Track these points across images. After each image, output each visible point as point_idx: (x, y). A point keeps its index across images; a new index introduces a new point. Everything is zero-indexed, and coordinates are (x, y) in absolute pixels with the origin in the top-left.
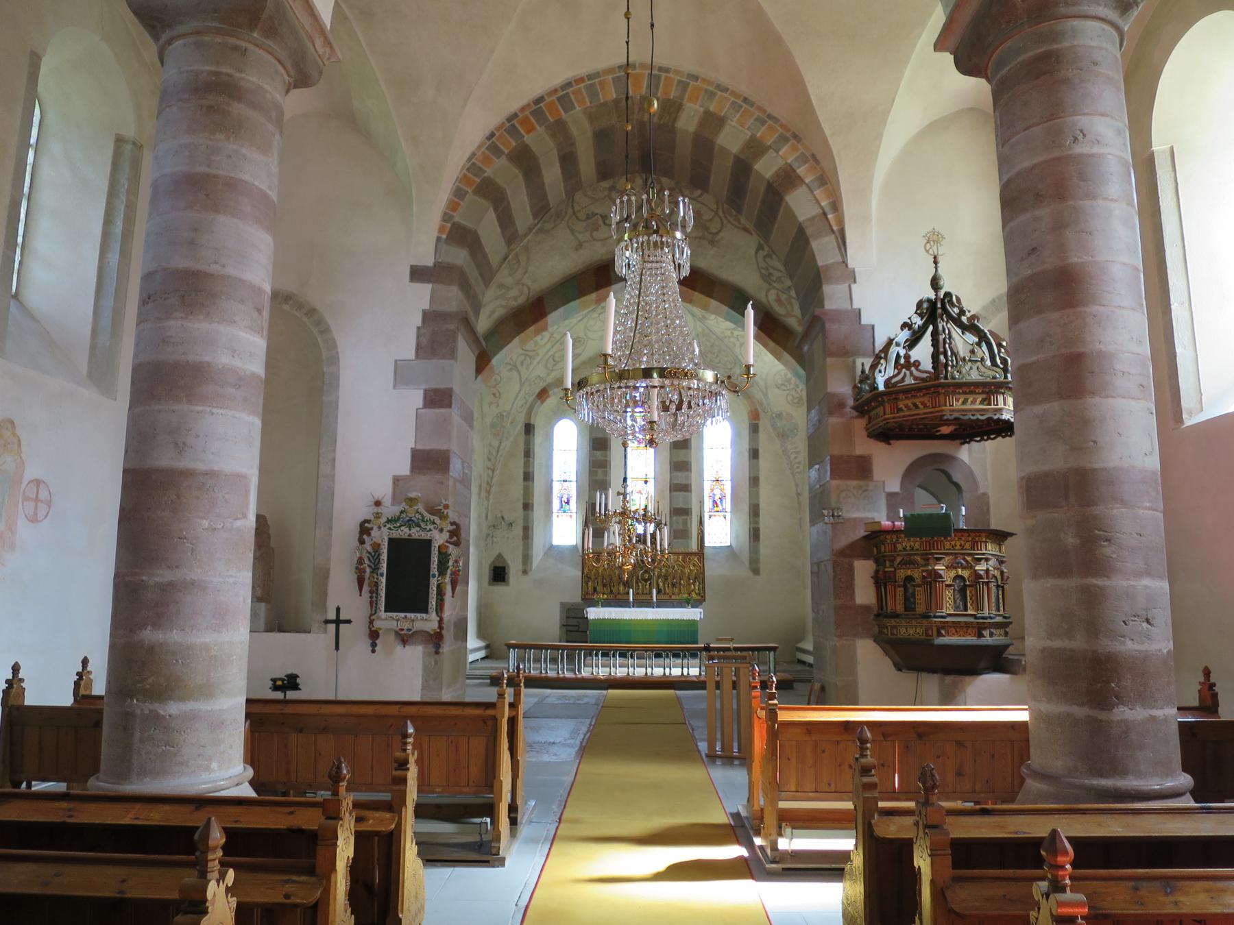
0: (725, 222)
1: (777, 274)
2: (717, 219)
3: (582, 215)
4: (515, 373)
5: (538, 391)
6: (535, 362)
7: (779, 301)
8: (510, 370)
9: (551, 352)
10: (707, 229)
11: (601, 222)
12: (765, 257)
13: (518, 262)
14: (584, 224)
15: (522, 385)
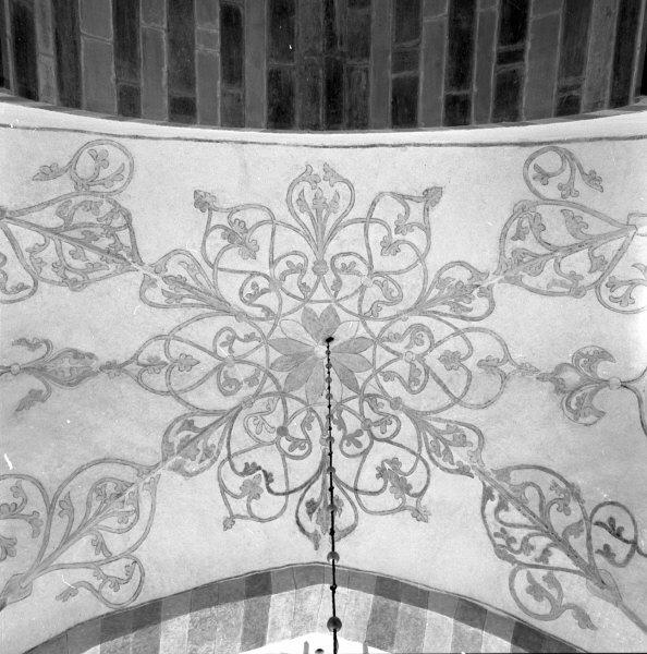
1: (519, 534)
3: (241, 468)
7: (534, 589)
10: (407, 488)
11: (263, 484)
12: (497, 510)
13: (137, 511)
14: (240, 480)
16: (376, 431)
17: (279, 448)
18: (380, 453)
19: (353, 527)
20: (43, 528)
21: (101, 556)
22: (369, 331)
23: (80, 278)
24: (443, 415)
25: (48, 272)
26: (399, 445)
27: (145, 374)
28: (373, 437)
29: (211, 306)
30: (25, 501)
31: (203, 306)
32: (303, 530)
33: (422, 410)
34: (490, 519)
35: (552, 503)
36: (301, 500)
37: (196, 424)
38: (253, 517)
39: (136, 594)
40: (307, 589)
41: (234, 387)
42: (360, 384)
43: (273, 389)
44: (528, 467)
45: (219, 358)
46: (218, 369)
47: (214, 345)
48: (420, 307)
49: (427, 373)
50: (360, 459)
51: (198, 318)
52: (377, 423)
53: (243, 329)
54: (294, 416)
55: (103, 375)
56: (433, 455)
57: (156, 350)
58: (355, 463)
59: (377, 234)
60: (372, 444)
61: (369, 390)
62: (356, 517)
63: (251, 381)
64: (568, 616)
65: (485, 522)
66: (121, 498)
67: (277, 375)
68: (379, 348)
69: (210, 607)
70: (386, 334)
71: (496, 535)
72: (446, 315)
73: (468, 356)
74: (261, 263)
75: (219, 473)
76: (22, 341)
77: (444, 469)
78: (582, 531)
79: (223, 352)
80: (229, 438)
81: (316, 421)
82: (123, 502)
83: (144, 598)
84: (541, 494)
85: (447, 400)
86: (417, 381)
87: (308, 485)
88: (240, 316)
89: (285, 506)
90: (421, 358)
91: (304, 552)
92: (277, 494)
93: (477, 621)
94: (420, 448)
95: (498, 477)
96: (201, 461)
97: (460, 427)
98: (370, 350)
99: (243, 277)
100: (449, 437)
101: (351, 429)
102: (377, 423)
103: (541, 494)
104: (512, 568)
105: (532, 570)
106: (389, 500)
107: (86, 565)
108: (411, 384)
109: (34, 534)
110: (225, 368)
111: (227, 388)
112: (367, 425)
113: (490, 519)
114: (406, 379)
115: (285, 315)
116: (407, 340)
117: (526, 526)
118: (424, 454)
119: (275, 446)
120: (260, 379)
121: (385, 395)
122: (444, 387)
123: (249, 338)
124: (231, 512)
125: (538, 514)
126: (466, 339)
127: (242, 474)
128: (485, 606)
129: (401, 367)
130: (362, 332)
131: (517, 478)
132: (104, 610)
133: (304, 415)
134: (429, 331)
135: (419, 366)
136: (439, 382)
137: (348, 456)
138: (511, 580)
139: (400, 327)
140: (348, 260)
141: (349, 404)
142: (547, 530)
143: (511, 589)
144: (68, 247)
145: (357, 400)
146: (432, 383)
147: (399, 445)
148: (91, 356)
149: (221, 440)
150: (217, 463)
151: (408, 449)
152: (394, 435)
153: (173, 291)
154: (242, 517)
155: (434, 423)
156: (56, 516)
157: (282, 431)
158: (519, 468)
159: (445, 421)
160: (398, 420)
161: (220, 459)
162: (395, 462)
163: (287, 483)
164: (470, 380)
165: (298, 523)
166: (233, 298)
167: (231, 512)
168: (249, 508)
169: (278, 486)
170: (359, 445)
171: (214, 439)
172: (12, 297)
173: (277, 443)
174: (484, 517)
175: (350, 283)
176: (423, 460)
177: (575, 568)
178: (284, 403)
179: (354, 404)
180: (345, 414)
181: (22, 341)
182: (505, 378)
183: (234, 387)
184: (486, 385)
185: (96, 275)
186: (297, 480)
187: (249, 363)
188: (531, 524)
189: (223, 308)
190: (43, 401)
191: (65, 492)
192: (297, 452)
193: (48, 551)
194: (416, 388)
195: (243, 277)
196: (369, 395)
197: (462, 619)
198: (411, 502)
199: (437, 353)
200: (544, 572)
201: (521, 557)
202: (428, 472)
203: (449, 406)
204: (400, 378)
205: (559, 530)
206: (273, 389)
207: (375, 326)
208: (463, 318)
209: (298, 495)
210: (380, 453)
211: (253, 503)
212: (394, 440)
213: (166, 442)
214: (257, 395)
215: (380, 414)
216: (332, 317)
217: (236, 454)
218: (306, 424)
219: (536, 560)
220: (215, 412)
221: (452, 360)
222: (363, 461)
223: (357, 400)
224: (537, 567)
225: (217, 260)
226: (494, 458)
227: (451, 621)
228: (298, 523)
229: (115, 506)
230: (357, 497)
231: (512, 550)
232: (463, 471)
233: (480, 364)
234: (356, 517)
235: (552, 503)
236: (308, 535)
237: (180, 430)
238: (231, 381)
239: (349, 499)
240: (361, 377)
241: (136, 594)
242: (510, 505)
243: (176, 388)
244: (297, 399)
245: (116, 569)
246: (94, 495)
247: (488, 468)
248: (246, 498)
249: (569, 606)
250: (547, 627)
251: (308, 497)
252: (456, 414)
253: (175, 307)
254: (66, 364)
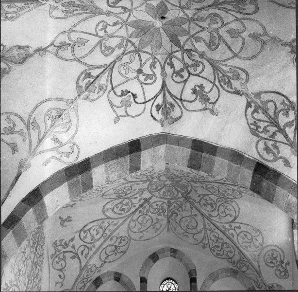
0: (221, 89)
1: (262, 125)
2: (215, 88)
3: (119, 93)
4: (76, 260)
5: (94, 278)
6: (91, 253)
7: (267, 149)
8: (73, 258)
9: (104, 246)
11: (132, 99)
13: (70, 122)
14: (120, 99)
15: (81, 270)
16: (191, 70)
17: (139, 80)
18: (194, 82)
19: (180, 117)
20: (27, 137)
21: (58, 145)
22: (186, 15)
23: (14, 15)
24: (227, 63)
26: (203, 78)
27: (60, 51)
28: (189, 73)
29: (92, 12)
30: (14, 125)
31: (86, 13)
32: (155, 119)
33: (217, 59)
34: (249, 116)
35: (281, 111)
36: (153, 105)
37: (92, 74)
38: (128, 115)
39: (77, 157)
40: (159, 147)
41: (110, 51)
42: (182, 44)
43: (132, 49)
44: (271, 92)
45: (100, 37)
46: (100, 43)
47: (96, 31)
49: (219, 39)
50: (183, 84)
51: (86, 19)
52: (191, 66)
53: (111, 20)
54: (145, 62)
55: (36, 55)
56: (222, 83)
57: (64, 38)
58: (180, 86)
60: (189, 77)
61: (186, 47)
62: (182, 112)
63: (119, 46)
64: (281, 161)
65: (246, 117)
66: (61, 117)
67: (133, 40)
68: (192, 24)
69: (113, 160)
70: (196, 17)
71: (251, 124)
72: (231, 10)
73: (243, 32)
75: (108, 97)
77: (227, 91)
78: (293, 125)
79: (102, 33)
80: (111, 79)
81: (158, 63)
82: (62, 119)
83: (81, 159)
84: (275, 106)
85: (230, 54)
86: (214, 44)
87: (156, 97)
88: (108, 14)
89: (145, 109)
90: (217, 30)
91: (156, 129)
92: (140, 103)
93: (238, 162)
94: (215, 79)
95: (255, 97)
96: (98, 92)
97: (237, 69)
98: (187, 25)
100: (230, 75)
101: (178, 68)
102: (191, 66)
103: (275, 106)
104: (258, 139)
105: (266, 141)
106: (198, 105)
107: (53, 149)
108: (212, 45)
109: (24, 140)
110: (104, 42)
111: (106, 52)
112: (186, 66)
113: (249, 116)
114: (208, 41)
115: (135, 8)
116: (208, 21)
117: (266, 121)
118: (217, 83)
119: (136, 79)
120: (124, 44)
121: (196, 51)
122: (229, 48)
123: (115, 24)
124: (117, 115)
125: (273, 116)
126: (243, 24)
127: (120, 96)
128: (244, 154)
129: (205, 35)
130: (181, 14)
131: (265, 97)
132: (65, 166)
133: (151, 61)
134: (221, 18)
135: (215, 35)
136: (227, 44)
137: (176, 82)
138: (257, 144)
139: (204, 14)
141: (175, 54)
142: (275, 123)
143: (257, 148)
145: (180, 52)
146: (222, 45)
147: (203, 78)
148: (28, 47)
149: (107, 80)
150: (107, 92)
151: (209, 80)
152: (201, 72)
153: (68, 9)
154: (123, 116)
155: (223, 67)
156: (31, 130)
157: (140, 71)
158: (266, 92)
159: (229, 66)
160: (203, 64)
161: (108, 90)
162: (201, 87)
163: (145, 98)
164: (243, 44)
165: (152, 116)
167: (117, 115)
168: (126, 112)
169: (140, 99)
170: (182, 77)
171: (103, 80)
173: (137, 77)
174: (246, 115)
176: (216, 86)
177: (286, 142)
178: (139, 56)
179: (179, 55)
180: (174, 60)
182: (264, 43)
183: (110, 51)
184: (253, 47)
185: (23, 12)
186: (150, 94)
187: (117, 36)
188: (269, 121)
190: (8, 74)
191: (32, 118)
192: (149, 81)
193: (33, 148)
194: (213, 47)
196: (187, 50)
197: (232, 161)
198: (210, 106)
199: (225, 29)
200: (273, 142)
201: (262, 135)
202: (219, 92)
203: (231, 58)
204: (204, 41)
205: (282, 124)
206: (132, 49)
208: (241, 13)
209: (151, 102)
210: (194, 82)
211: (128, 109)
212: (201, 75)
213: (78, 86)
214: (123, 54)
215: (193, 60)
216: (164, 7)
217: (116, 86)
218: (152, 66)
219: (269, 136)
220: (101, 67)
221: (234, 33)
222: (185, 85)
223: (180, 52)
224: (269, 140)
226: (254, 87)
227: (227, 161)
228: (152, 116)
229: (59, 121)
230: (182, 103)
231: (258, 131)
232: (237, 92)
233: (250, 36)
234: (182, 112)
235: (281, 111)
236: (157, 121)
237: (84, 79)
238: (108, 48)
239: (178, 104)
240: (182, 39)
241: (77, 157)
242: (259, 111)
243: (78, 57)
244: (147, 53)
245: (66, 148)
246: (47, 118)
247: (250, 92)
248: (124, 107)
249: (281, 157)
250: (271, 165)
251: (156, 103)
252: (236, 62)
253: (70, 16)
254: (15, 52)
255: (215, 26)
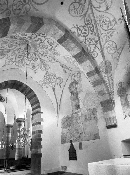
22: (20, 46)
25: (56, 79)
48: (9, 50)
51: (44, 61)
53: (40, 55)
57: (53, 61)
59: (14, 60)
74: (32, 62)
76: (66, 72)
79: (45, 54)
99: (36, 61)
130: (21, 46)
139: (14, 47)
140: (20, 57)
144: (51, 80)
166: (39, 60)
172: (61, 79)
175: (20, 54)
181: (66, 72)
185: (52, 74)
189: (41, 59)
195: (36, 61)
207: (18, 47)
208: (2, 50)
225: (37, 66)
255: (12, 44)
